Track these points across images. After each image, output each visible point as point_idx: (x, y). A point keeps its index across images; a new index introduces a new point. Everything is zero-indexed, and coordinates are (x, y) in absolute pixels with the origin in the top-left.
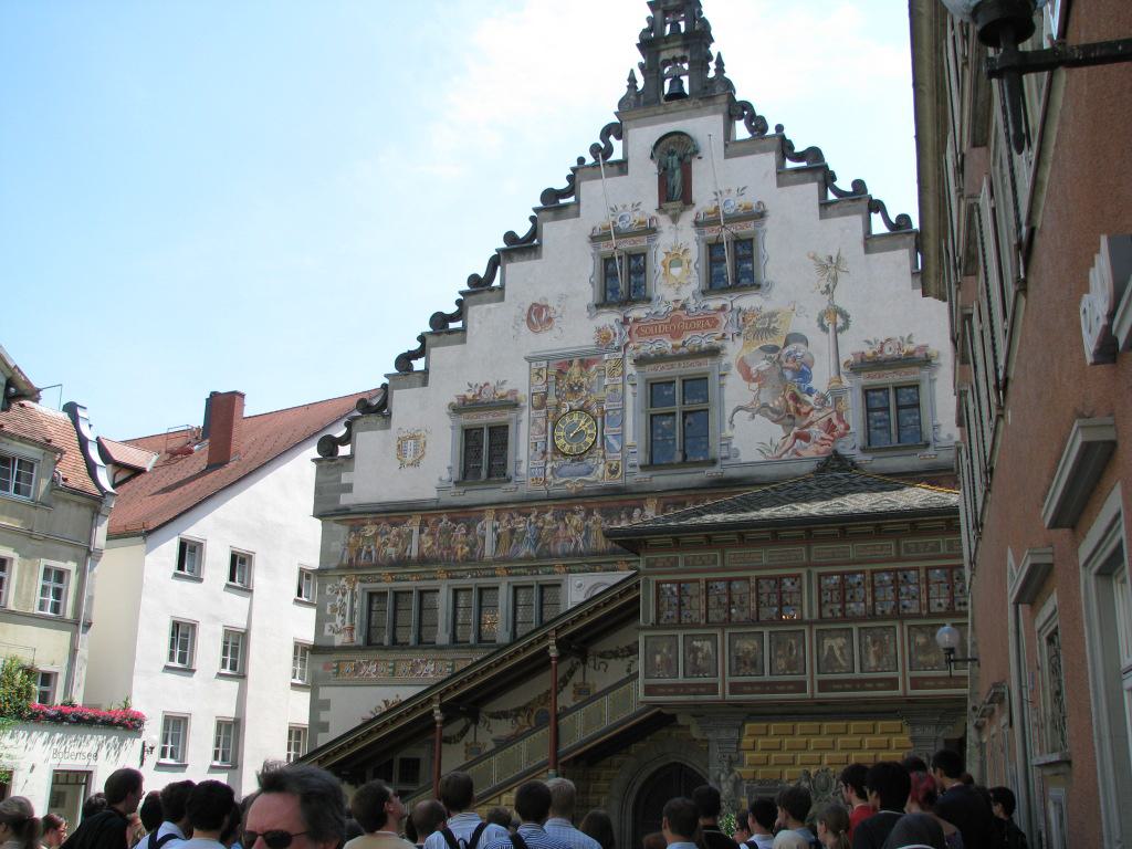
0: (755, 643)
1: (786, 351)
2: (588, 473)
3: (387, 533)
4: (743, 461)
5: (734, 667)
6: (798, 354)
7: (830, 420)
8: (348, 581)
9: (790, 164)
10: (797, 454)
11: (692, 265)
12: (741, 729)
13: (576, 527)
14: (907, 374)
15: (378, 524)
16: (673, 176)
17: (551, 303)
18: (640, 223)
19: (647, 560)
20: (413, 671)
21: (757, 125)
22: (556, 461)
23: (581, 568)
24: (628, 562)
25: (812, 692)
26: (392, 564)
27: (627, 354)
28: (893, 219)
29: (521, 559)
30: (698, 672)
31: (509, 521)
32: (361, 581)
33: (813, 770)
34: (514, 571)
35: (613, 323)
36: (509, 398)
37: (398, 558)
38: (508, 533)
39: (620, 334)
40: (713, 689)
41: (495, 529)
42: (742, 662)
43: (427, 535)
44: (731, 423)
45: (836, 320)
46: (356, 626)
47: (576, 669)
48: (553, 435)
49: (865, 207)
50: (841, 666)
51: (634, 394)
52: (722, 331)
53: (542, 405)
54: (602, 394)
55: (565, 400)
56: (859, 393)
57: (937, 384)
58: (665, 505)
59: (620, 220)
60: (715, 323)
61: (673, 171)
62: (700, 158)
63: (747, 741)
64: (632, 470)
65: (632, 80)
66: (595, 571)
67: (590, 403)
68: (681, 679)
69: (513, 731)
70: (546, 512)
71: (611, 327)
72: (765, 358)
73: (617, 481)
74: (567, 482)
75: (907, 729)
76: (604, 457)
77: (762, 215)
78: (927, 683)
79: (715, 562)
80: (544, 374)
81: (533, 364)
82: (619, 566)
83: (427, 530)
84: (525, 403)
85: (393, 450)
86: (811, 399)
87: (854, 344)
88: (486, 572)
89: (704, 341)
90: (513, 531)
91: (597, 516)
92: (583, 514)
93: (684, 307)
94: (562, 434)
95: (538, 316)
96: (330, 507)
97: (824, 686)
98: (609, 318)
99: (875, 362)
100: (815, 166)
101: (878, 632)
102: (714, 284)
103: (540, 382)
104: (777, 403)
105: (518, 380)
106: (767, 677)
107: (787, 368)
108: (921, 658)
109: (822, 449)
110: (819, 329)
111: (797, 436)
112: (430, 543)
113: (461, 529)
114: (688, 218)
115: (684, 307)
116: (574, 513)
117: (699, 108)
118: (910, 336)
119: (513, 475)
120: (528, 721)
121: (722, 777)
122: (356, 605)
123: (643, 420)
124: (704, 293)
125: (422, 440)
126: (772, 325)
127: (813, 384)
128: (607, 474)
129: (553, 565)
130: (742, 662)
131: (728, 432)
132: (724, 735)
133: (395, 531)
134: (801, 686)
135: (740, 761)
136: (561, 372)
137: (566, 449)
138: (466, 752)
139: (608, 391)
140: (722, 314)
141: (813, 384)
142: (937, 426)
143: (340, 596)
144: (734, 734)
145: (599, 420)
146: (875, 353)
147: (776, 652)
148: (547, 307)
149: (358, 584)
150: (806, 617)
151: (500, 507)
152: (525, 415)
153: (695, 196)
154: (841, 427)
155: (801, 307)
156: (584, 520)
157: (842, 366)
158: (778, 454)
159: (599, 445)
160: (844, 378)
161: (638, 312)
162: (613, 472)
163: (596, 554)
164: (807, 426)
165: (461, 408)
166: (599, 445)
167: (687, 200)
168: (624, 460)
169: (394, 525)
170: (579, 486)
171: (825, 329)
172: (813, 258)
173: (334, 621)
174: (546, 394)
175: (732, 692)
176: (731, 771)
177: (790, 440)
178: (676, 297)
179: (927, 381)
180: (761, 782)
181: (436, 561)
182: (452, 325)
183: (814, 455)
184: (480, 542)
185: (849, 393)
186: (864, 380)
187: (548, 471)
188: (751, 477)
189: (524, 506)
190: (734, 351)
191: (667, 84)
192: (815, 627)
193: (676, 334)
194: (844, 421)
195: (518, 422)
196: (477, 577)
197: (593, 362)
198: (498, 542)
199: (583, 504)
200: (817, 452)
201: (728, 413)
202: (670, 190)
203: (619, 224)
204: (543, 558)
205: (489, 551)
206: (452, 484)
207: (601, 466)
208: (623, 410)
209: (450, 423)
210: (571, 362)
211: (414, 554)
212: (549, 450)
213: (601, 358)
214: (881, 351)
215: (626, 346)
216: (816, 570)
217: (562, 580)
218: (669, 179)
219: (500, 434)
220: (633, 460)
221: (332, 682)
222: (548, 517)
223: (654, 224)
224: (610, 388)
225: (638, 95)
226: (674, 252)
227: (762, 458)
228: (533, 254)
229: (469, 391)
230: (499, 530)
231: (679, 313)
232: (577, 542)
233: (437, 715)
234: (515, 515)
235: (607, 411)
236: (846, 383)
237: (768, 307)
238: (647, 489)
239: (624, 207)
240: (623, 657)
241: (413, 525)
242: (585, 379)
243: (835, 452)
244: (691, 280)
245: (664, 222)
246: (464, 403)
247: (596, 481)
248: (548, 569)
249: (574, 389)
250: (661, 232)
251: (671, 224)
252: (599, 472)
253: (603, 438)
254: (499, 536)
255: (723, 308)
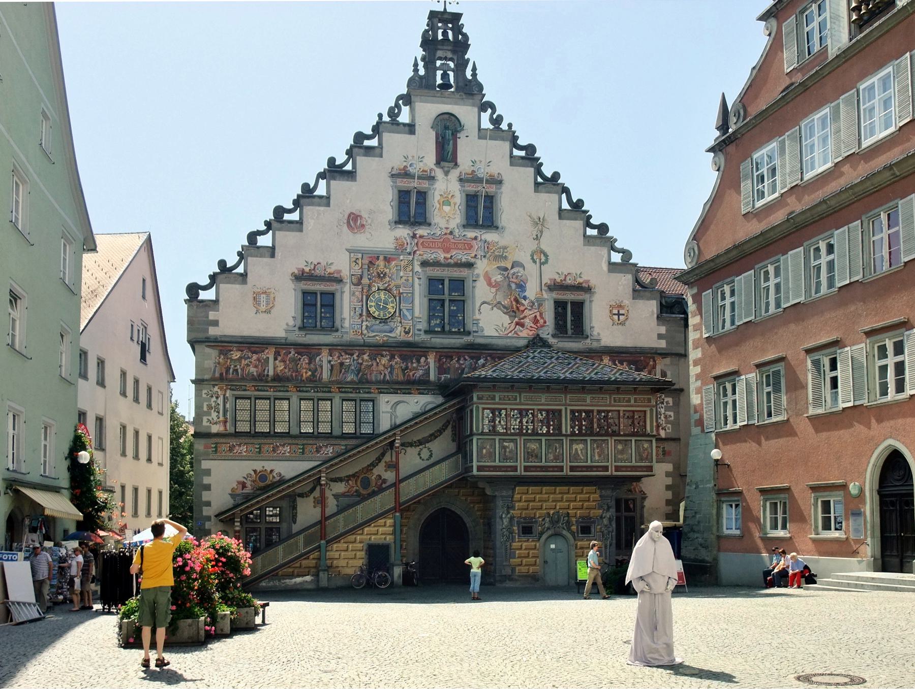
0: (537, 445)
1: (512, 271)
2: (391, 332)
3: (249, 358)
4: (486, 334)
5: (526, 457)
6: (519, 274)
7: (536, 316)
8: (221, 389)
9: (516, 152)
10: (517, 334)
11: (457, 207)
12: (514, 490)
13: (384, 365)
14: (578, 295)
15: (242, 351)
16: (449, 145)
17: (364, 215)
18: (423, 171)
19: (478, 395)
20: (274, 451)
21: (497, 121)
22: (369, 322)
23: (389, 391)
24: (418, 389)
25: (566, 472)
26: (254, 379)
27: (416, 258)
28: (575, 201)
29: (347, 382)
30: (507, 459)
31: (339, 357)
32: (230, 389)
33: (552, 512)
34: (343, 390)
35: (406, 236)
36: (335, 275)
37: (259, 375)
38: (339, 365)
39: (411, 244)
40: (515, 469)
41: (330, 362)
42: (529, 455)
43: (280, 361)
44: (479, 310)
45: (541, 257)
46: (228, 420)
47: (386, 452)
48: (367, 304)
49: (560, 190)
50: (581, 459)
51: (420, 285)
52: (475, 253)
53: (359, 283)
54: (399, 282)
55: (375, 282)
56: (552, 302)
57: (593, 303)
58: (440, 356)
59: (410, 166)
60: (471, 247)
61: (449, 140)
62: (467, 136)
63: (517, 497)
64: (419, 333)
65: (416, 65)
66: (397, 393)
67: (391, 287)
68: (497, 463)
69: (346, 490)
70: (364, 354)
71: (405, 238)
72: (500, 274)
73: (409, 338)
74: (377, 335)
75: (598, 491)
76: (401, 322)
77: (500, 182)
78: (578, 469)
79: (516, 399)
80: (360, 262)
81: (352, 254)
82: (413, 392)
83: (279, 358)
84: (347, 280)
85: (250, 301)
86: (525, 303)
87: (550, 274)
88: (324, 389)
89: (463, 256)
90: (342, 364)
91: (397, 359)
92: (389, 357)
93: (451, 233)
94: (373, 304)
95: (354, 221)
96: (201, 336)
97: (572, 469)
98: (403, 232)
99: (561, 286)
100: (530, 157)
101: (600, 442)
102: (471, 221)
103: (357, 267)
104: (506, 302)
105: (342, 264)
106: (543, 463)
107: (512, 282)
108: (619, 456)
109: (531, 333)
110: (531, 261)
111: (517, 324)
112: (283, 367)
113: (305, 360)
114: (454, 174)
115: (451, 233)
116: (382, 356)
117: (463, 99)
118: (581, 273)
119: (340, 327)
120: (356, 484)
121: (503, 516)
122: (228, 406)
123: (425, 301)
124: (464, 226)
125: (272, 296)
126: (505, 254)
127: (526, 294)
128: (403, 333)
129: (370, 388)
130: (529, 455)
131: (477, 316)
132: (504, 493)
133: (255, 357)
134: (561, 469)
135: (513, 508)
136: (371, 263)
137: (376, 315)
138: (314, 502)
139: (403, 280)
140: (475, 241)
141: (526, 294)
142: (592, 327)
143: (214, 399)
144: (510, 493)
145: (397, 298)
146: (561, 280)
147: (548, 450)
148: (361, 217)
149: (228, 391)
150: (564, 432)
151: (333, 348)
152: (347, 288)
153: (459, 160)
154: (541, 321)
155: (521, 245)
156: (390, 360)
157: (543, 285)
158: (506, 333)
159: (397, 314)
160: (544, 292)
161: (422, 231)
162: (407, 333)
163: (397, 383)
164: (523, 319)
165: (300, 277)
166: (397, 314)
167: (456, 164)
168: (414, 326)
169: (254, 352)
170: (385, 339)
171: (535, 262)
172: (530, 216)
173: (211, 416)
174: (361, 277)
175: (525, 471)
176: (508, 513)
177: (513, 325)
178: (447, 226)
179: (588, 301)
180: (525, 518)
181: (288, 379)
182: (287, 217)
183: (526, 336)
184: (319, 369)
185: (546, 302)
186: (555, 295)
187: (364, 327)
188: (490, 345)
189: (348, 348)
190: (482, 266)
191: (439, 73)
192: (569, 438)
193: (447, 250)
194: (542, 317)
195: (342, 293)
196: (317, 392)
197: (394, 259)
198: (331, 370)
199: (389, 351)
200: (528, 335)
201: (478, 305)
202: (446, 153)
203: (409, 168)
204: (363, 383)
205: (325, 375)
206: (296, 329)
207: (399, 328)
208: (413, 293)
209: (293, 286)
210: (378, 258)
211: (271, 373)
212: (364, 313)
213: (398, 258)
214: (565, 280)
215: (415, 252)
216: (569, 408)
217: (376, 398)
218: (446, 146)
219: (329, 302)
220: (419, 326)
221: (211, 457)
222: (366, 357)
223: (433, 174)
224: (404, 278)
225: (421, 77)
226: (445, 196)
227: (498, 335)
228: (350, 179)
229: (306, 266)
230: (332, 363)
231: (450, 237)
232: (385, 374)
233: (323, 480)
234: (343, 354)
235: (402, 293)
236: (545, 296)
237: (502, 243)
238: (428, 345)
239: (413, 157)
240: (416, 446)
241: (270, 354)
242: (388, 270)
243: (538, 335)
244: (456, 216)
245: (439, 173)
246: (303, 274)
247: (395, 337)
248: (367, 390)
249: (381, 276)
250: (438, 180)
251: (443, 176)
252: (398, 332)
253: (400, 310)
254: (332, 366)
255: (476, 238)
